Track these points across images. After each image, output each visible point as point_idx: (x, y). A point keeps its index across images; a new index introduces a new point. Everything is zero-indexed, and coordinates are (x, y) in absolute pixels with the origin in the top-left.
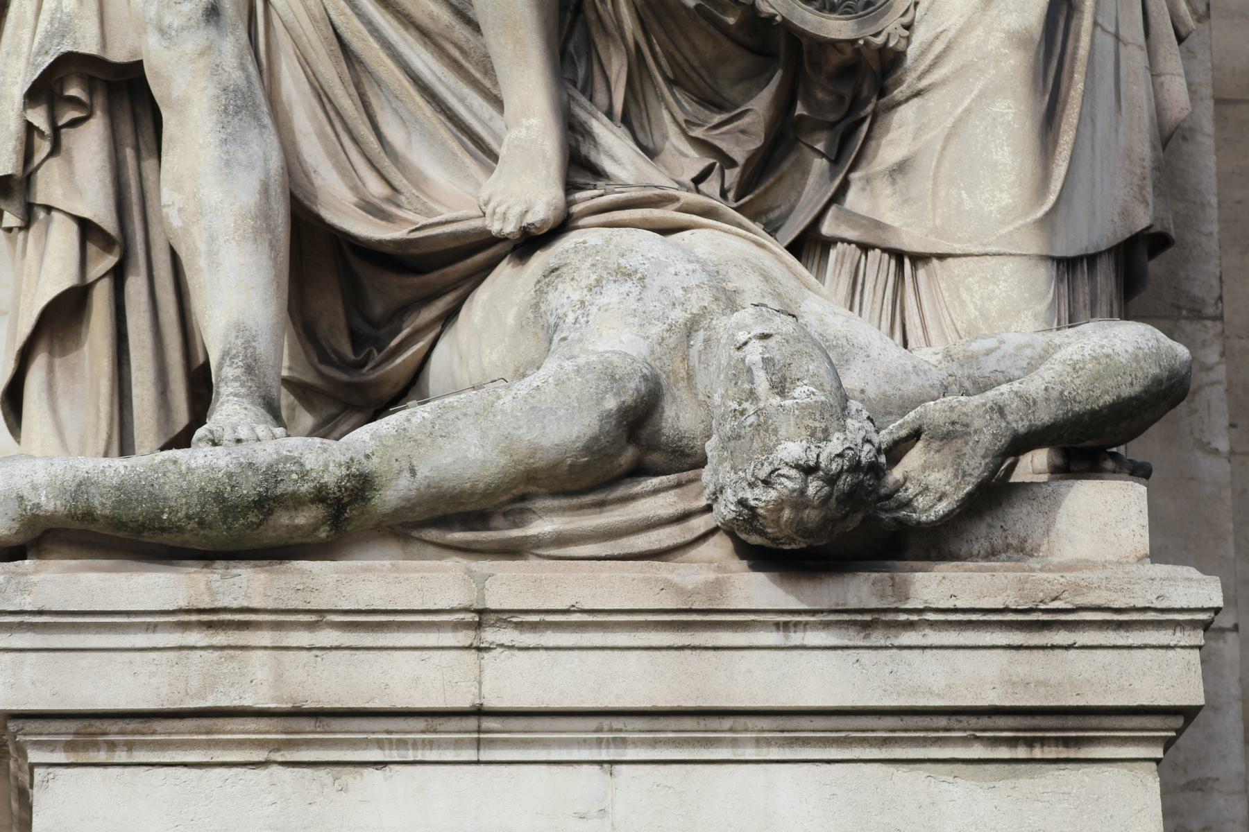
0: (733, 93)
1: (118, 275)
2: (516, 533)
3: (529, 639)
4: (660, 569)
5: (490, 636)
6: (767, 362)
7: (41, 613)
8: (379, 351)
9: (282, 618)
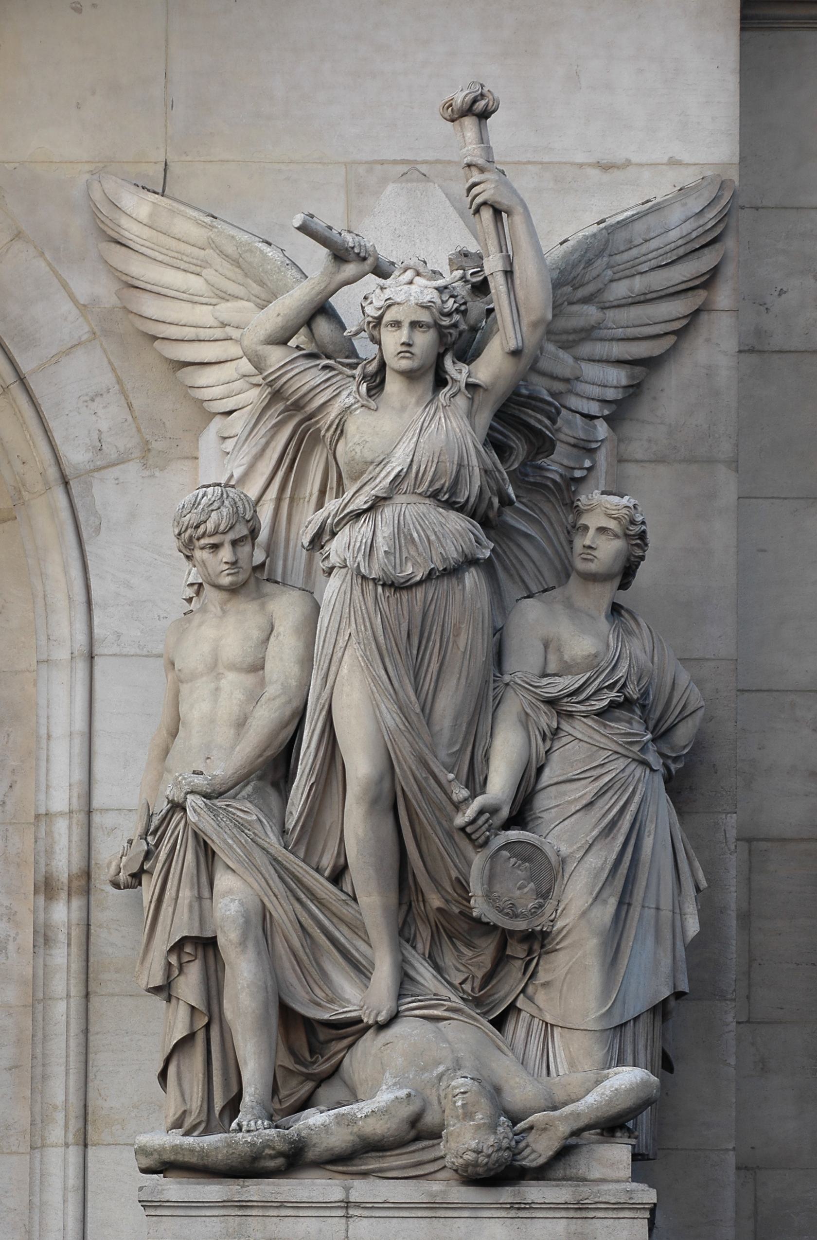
0: (477, 942)
1: (208, 1027)
2: (363, 1167)
3: (366, 1213)
4: (424, 1184)
5: (351, 1212)
6: (463, 1105)
7: (168, 1201)
8: (322, 1057)
9: (265, 1205)
